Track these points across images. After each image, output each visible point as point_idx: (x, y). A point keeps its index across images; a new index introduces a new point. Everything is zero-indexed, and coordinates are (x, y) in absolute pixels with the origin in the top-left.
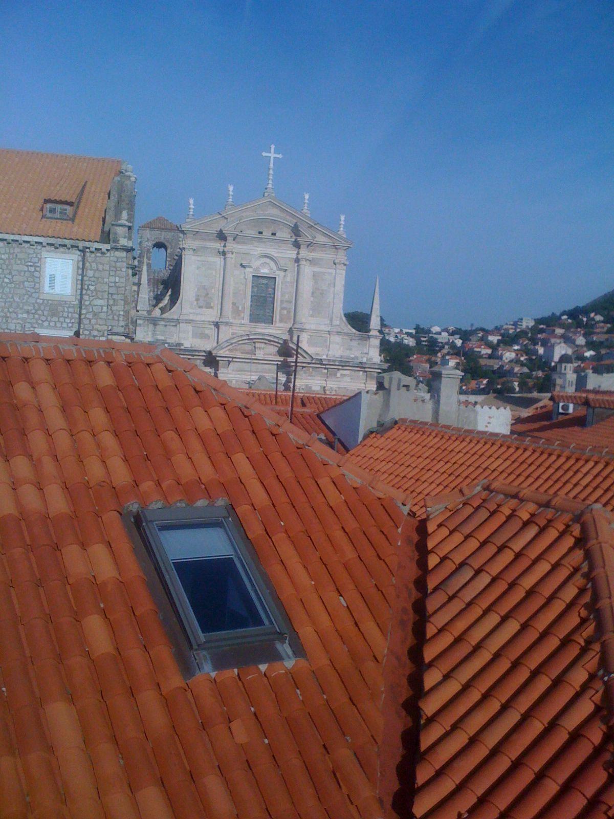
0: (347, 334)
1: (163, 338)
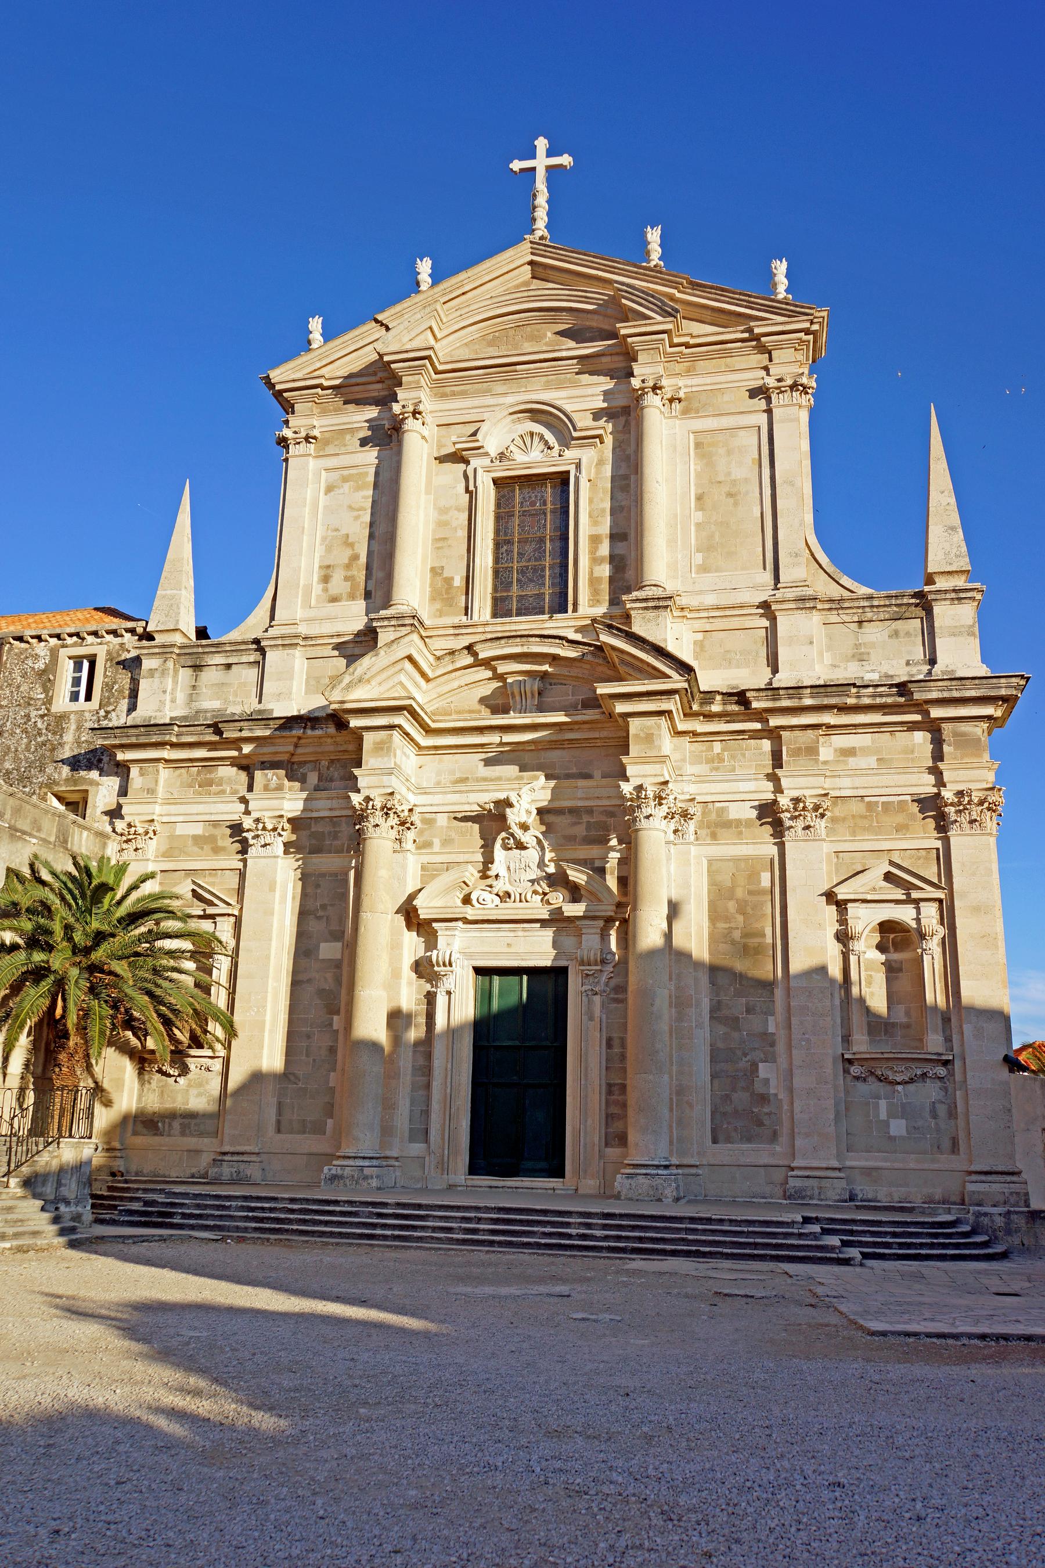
0: (836, 604)
1: (215, 704)
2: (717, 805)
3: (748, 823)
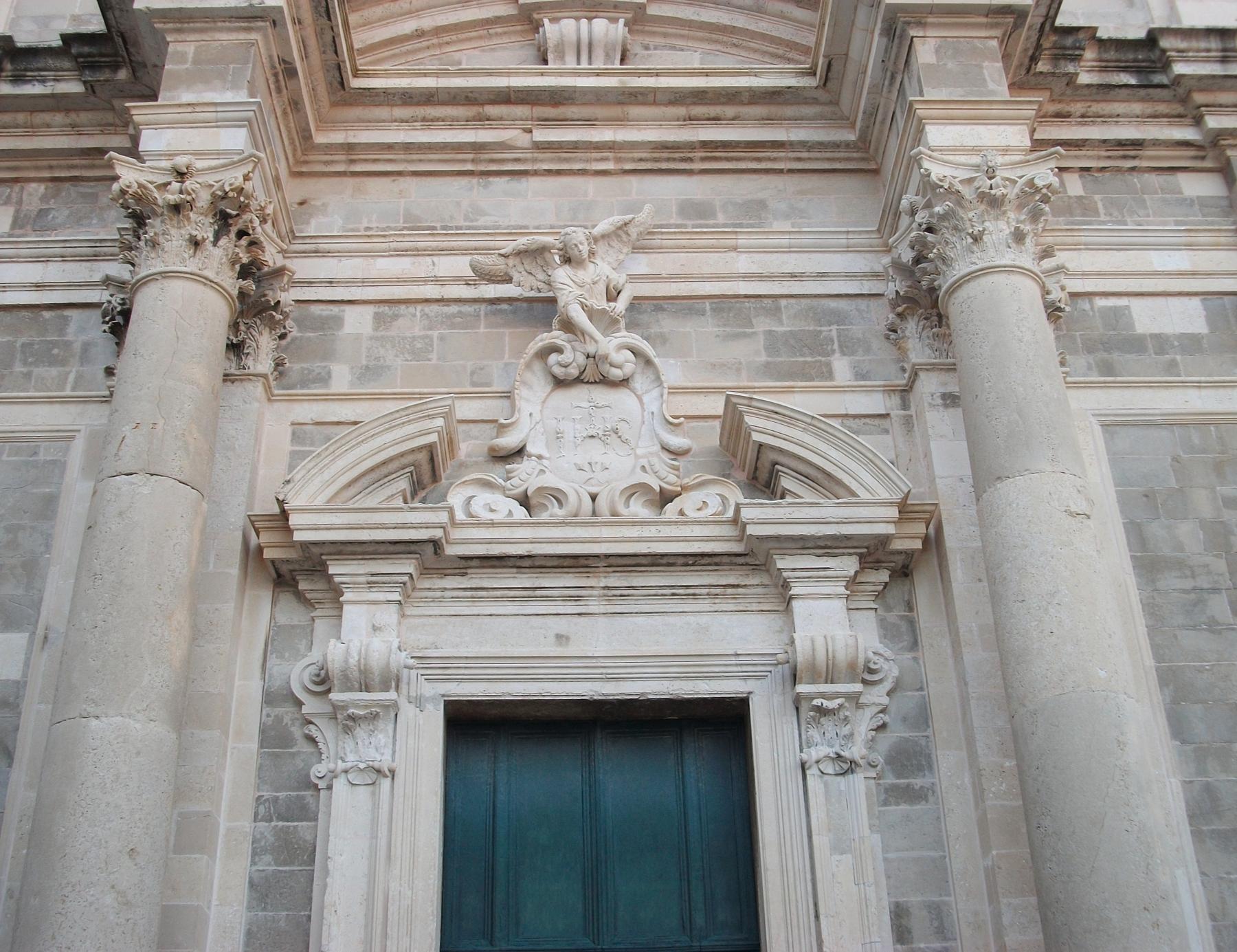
2: (1100, 302)
3: (1191, 343)
